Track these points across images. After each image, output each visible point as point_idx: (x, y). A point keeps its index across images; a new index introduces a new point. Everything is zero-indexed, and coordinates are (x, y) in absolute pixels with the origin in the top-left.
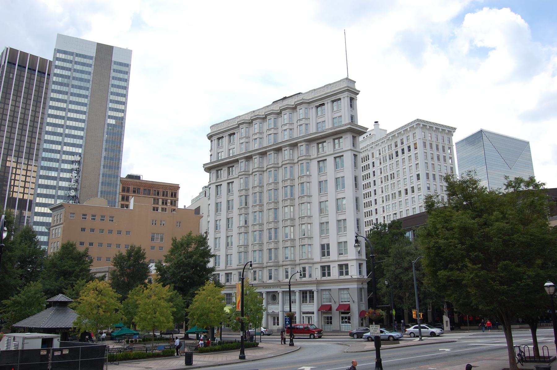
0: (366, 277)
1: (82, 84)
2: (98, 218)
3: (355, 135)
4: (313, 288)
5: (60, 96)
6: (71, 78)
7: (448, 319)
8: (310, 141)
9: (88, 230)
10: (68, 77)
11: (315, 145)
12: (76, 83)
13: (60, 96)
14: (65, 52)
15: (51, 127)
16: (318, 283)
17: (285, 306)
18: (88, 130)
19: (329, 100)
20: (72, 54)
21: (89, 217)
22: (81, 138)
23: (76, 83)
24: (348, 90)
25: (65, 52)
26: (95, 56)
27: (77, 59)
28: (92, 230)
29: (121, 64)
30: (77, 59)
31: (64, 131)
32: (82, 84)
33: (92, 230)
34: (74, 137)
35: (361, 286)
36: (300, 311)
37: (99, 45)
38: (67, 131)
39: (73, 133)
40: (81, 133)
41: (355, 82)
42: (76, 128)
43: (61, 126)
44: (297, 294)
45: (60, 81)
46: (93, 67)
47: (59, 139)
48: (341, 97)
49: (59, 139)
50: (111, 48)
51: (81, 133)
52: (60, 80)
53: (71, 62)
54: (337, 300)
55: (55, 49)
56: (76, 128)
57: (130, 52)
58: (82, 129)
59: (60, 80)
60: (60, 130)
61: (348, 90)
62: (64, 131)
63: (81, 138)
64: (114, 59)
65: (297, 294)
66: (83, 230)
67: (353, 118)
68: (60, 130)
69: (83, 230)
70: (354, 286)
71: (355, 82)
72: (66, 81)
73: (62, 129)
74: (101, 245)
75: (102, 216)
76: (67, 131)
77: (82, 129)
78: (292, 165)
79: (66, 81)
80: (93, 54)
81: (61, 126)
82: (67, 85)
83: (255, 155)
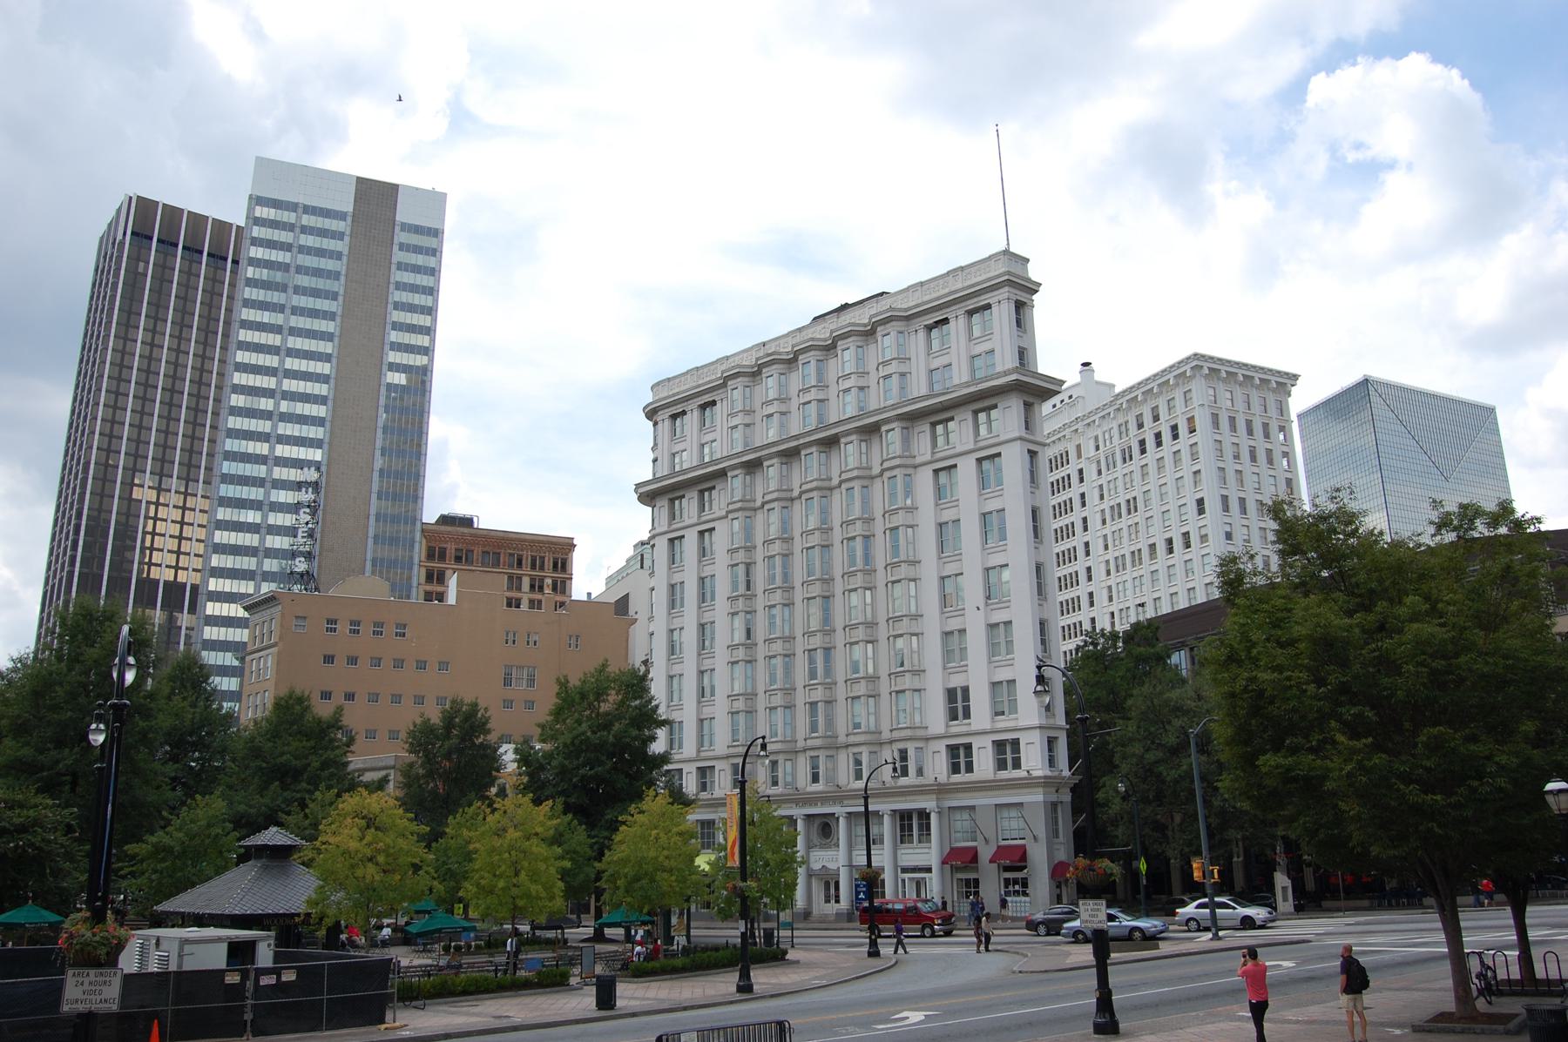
0: (1066, 773)
1: (321, 283)
2: (366, 629)
3: (1031, 400)
4: (928, 804)
5: (266, 317)
6: (293, 270)
8: (911, 418)
9: (340, 661)
10: (284, 267)
11: (927, 428)
12: (304, 281)
13: (266, 317)
14: (276, 204)
15: (242, 397)
16: (941, 790)
18: (337, 402)
19: (960, 310)
20: (292, 207)
21: (343, 628)
22: (318, 422)
23: (304, 281)
24: (1009, 283)
25: (276, 204)
26: (351, 209)
27: (307, 220)
28: (353, 660)
29: (418, 230)
30: (307, 220)
31: (277, 405)
32: (321, 283)
33: (353, 660)
35: (1054, 798)
36: (896, 866)
37: (360, 180)
38: (284, 406)
39: (299, 411)
40: (319, 411)
41: (1028, 260)
43: (269, 393)
44: (887, 819)
46: (347, 239)
47: (264, 426)
49: (264, 426)
50: (393, 189)
51: (319, 411)
52: (264, 274)
53: (290, 227)
54: (992, 837)
57: (442, 197)
58: (322, 400)
59: (264, 274)
60: (266, 404)
61: (1009, 283)
62: (277, 405)
63: (318, 422)
64: (402, 216)
65: (887, 819)
66: (329, 659)
67: (1024, 355)
68: (266, 404)
69: (329, 659)
70: (1037, 797)
71: (1028, 260)
72: (279, 276)
73: (271, 401)
74: (374, 698)
75: (376, 624)
76: (284, 406)
77: (322, 400)
78: (865, 483)
79: (279, 276)
80: (348, 207)
81: (269, 393)
82: (282, 288)
83: (770, 456)
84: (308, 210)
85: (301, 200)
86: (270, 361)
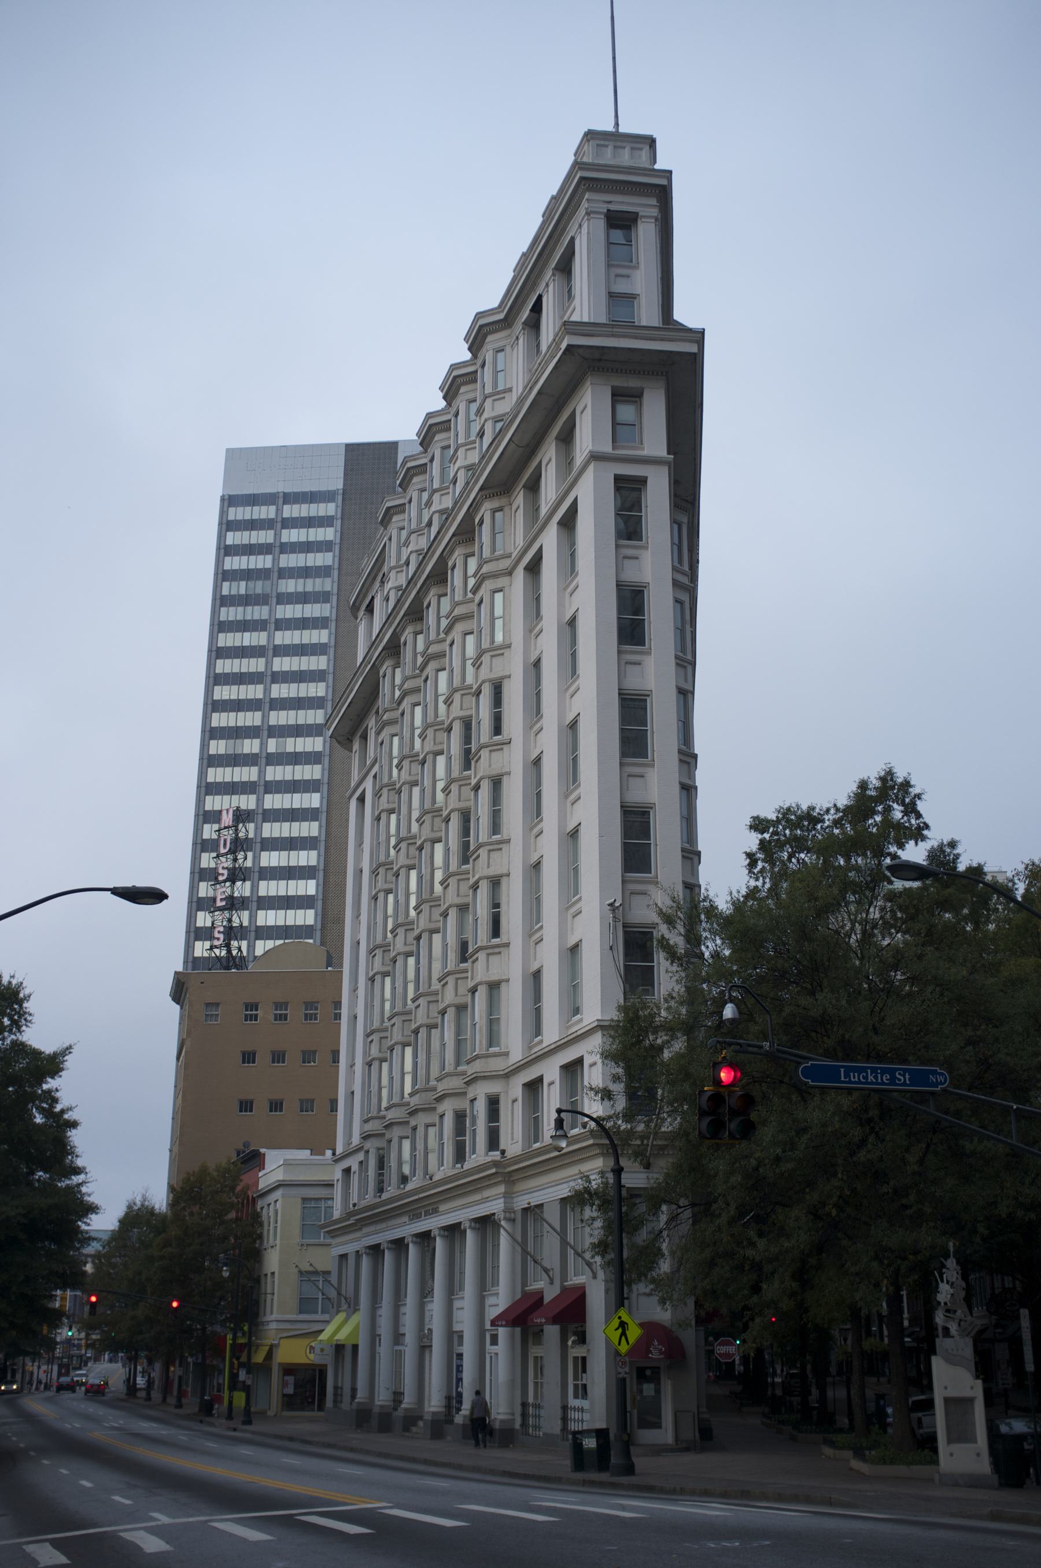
1: (310, 585)
3: (632, 383)
5: (248, 639)
7: (973, 1388)
9: (263, 1058)
10: (263, 574)
12: (290, 586)
13: (248, 639)
14: (253, 500)
17: (457, 1304)
19: (548, 274)
23: (290, 586)
25: (253, 500)
26: (340, 486)
27: (290, 511)
28: (278, 1057)
30: (290, 511)
31: (263, 745)
32: (310, 585)
33: (278, 1057)
34: (296, 759)
38: (272, 746)
39: (290, 749)
41: (651, 142)
42: (297, 731)
43: (251, 732)
45: (243, 592)
46: (338, 523)
48: (571, 234)
55: (223, 499)
56: (297, 731)
60: (250, 746)
65: (470, 1236)
66: (249, 1057)
68: (250, 746)
69: (249, 1057)
71: (651, 142)
72: (259, 587)
73: (256, 742)
75: (278, 1005)
76: (272, 746)
79: (259, 587)
80: (335, 481)
81: (251, 732)
82: (261, 600)
84: (290, 498)
85: (281, 488)
86: (253, 692)
